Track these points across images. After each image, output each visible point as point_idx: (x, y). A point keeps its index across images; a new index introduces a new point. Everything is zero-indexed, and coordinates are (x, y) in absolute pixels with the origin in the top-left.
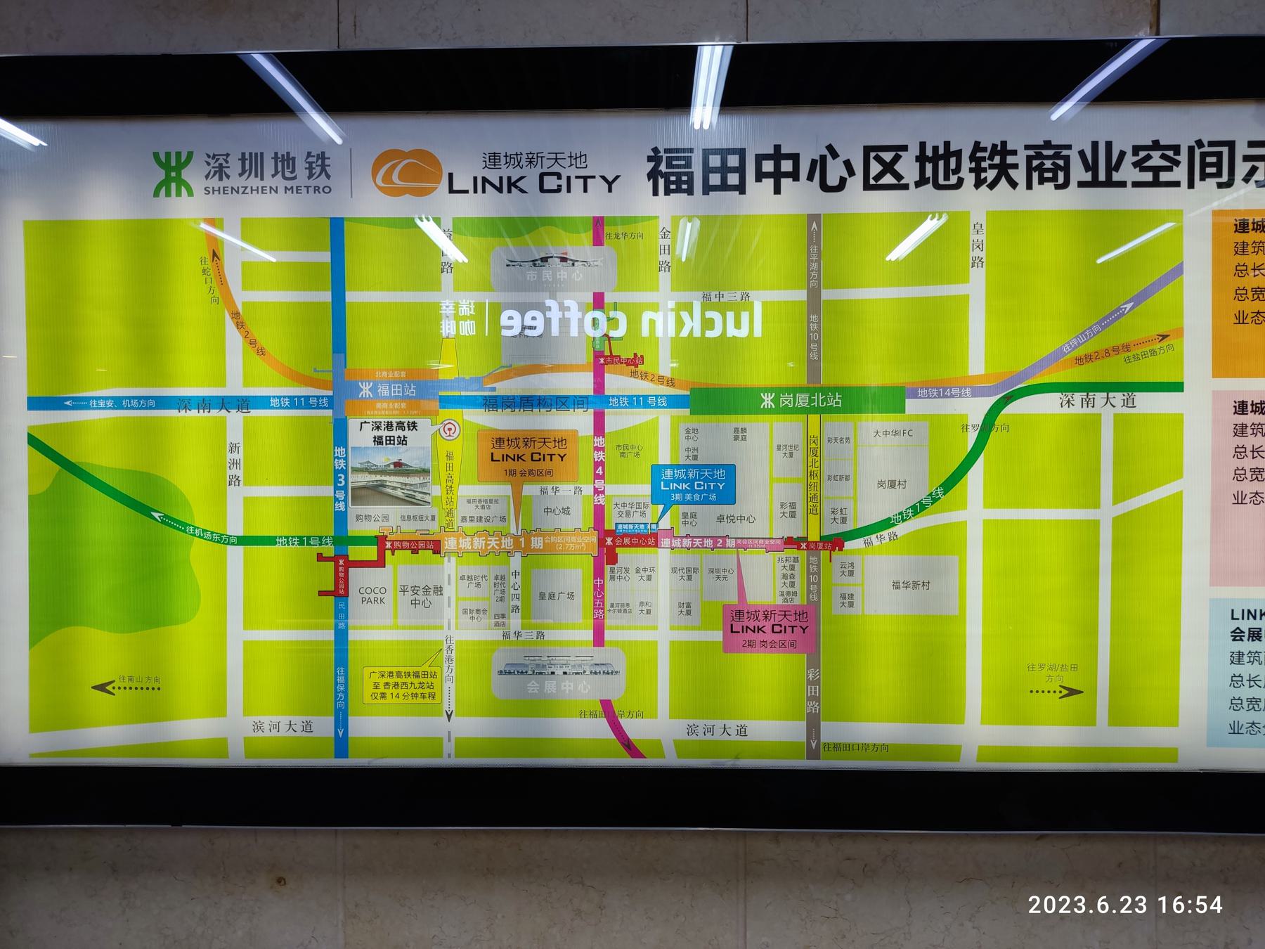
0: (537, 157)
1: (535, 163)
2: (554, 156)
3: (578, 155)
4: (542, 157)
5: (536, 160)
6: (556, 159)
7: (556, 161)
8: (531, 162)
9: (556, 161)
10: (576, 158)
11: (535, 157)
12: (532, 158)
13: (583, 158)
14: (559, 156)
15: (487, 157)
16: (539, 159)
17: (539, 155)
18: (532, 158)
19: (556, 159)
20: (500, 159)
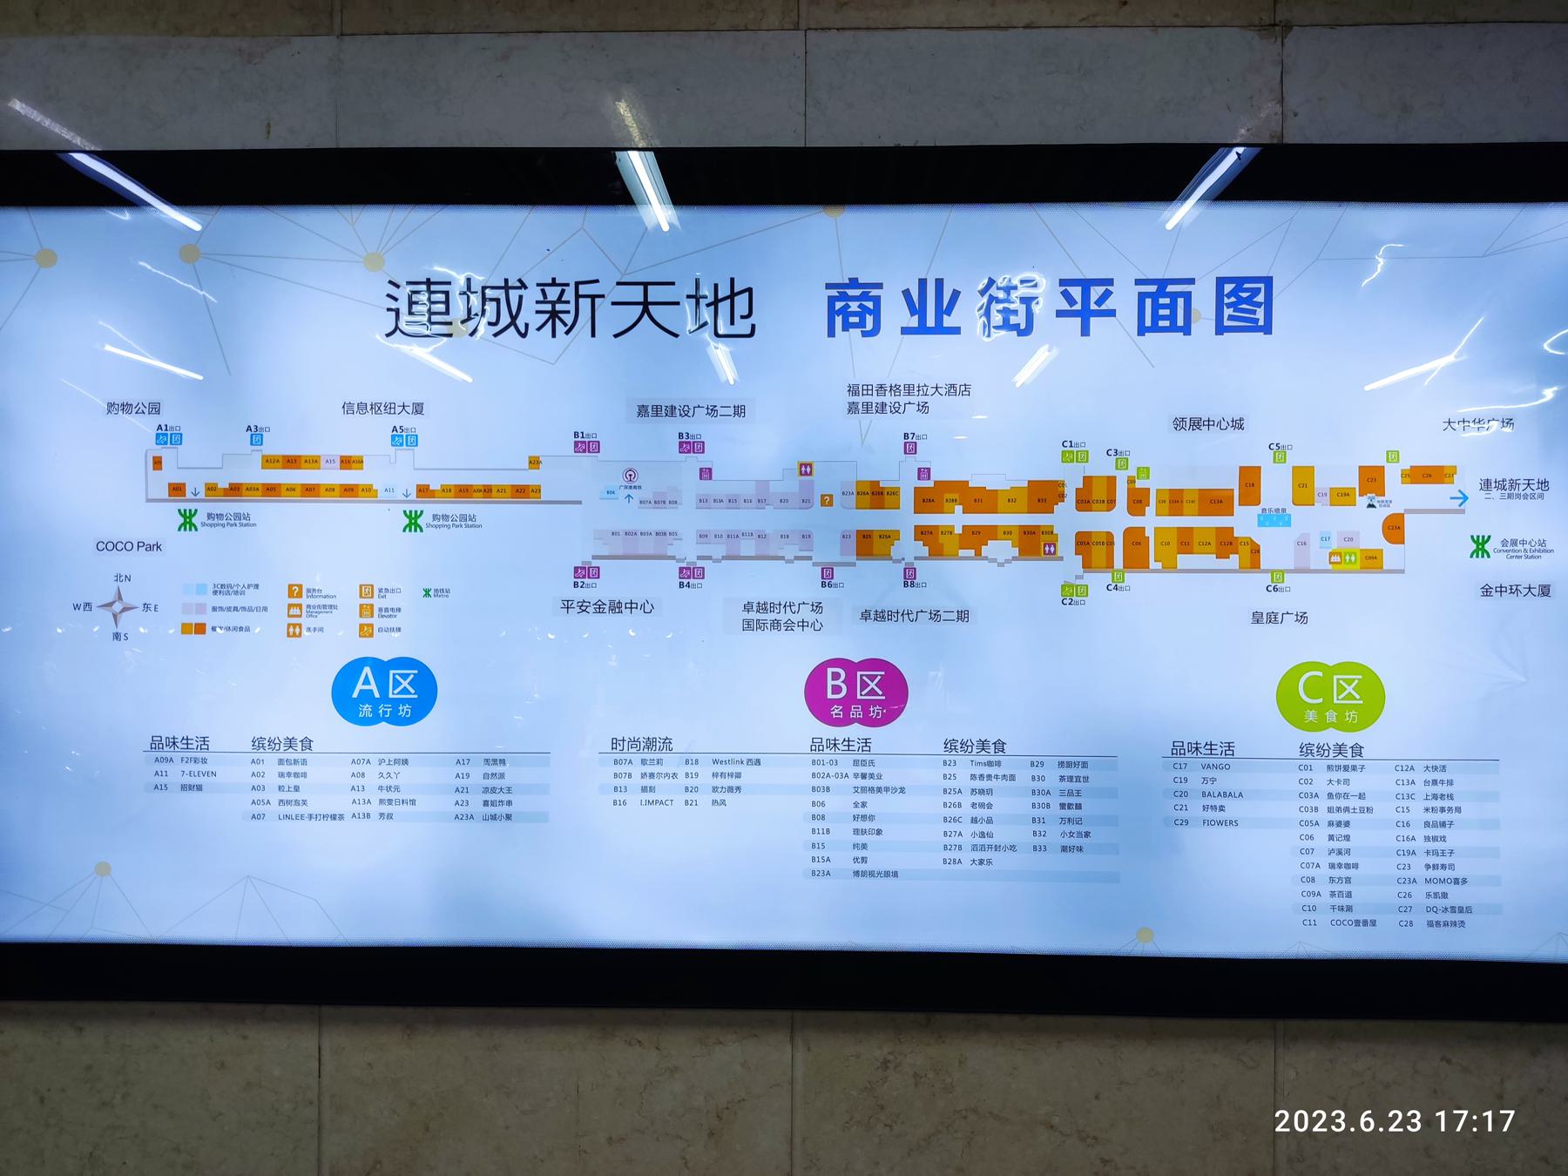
0: (578, 296)
1: (569, 319)
2: (636, 294)
3: (724, 291)
4: (593, 297)
5: (572, 307)
6: (646, 304)
7: (646, 311)
8: (554, 315)
9: (646, 311)
10: (715, 303)
11: (569, 294)
12: (560, 300)
13: (741, 303)
14: (655, 294)
15: (403, 293)
16: (585, 304)
17: (583, 290)
18: (560, 300)
19: (646, 304)
20: (447, 303)
